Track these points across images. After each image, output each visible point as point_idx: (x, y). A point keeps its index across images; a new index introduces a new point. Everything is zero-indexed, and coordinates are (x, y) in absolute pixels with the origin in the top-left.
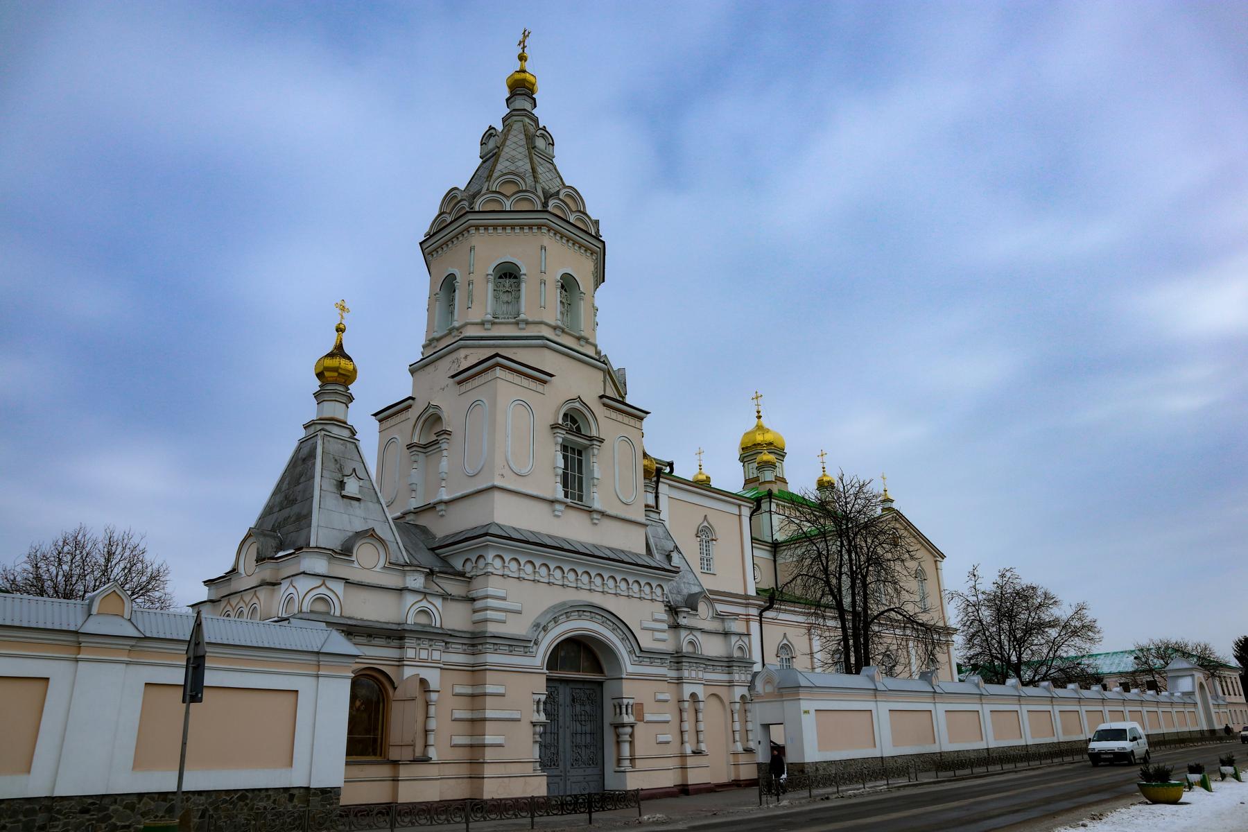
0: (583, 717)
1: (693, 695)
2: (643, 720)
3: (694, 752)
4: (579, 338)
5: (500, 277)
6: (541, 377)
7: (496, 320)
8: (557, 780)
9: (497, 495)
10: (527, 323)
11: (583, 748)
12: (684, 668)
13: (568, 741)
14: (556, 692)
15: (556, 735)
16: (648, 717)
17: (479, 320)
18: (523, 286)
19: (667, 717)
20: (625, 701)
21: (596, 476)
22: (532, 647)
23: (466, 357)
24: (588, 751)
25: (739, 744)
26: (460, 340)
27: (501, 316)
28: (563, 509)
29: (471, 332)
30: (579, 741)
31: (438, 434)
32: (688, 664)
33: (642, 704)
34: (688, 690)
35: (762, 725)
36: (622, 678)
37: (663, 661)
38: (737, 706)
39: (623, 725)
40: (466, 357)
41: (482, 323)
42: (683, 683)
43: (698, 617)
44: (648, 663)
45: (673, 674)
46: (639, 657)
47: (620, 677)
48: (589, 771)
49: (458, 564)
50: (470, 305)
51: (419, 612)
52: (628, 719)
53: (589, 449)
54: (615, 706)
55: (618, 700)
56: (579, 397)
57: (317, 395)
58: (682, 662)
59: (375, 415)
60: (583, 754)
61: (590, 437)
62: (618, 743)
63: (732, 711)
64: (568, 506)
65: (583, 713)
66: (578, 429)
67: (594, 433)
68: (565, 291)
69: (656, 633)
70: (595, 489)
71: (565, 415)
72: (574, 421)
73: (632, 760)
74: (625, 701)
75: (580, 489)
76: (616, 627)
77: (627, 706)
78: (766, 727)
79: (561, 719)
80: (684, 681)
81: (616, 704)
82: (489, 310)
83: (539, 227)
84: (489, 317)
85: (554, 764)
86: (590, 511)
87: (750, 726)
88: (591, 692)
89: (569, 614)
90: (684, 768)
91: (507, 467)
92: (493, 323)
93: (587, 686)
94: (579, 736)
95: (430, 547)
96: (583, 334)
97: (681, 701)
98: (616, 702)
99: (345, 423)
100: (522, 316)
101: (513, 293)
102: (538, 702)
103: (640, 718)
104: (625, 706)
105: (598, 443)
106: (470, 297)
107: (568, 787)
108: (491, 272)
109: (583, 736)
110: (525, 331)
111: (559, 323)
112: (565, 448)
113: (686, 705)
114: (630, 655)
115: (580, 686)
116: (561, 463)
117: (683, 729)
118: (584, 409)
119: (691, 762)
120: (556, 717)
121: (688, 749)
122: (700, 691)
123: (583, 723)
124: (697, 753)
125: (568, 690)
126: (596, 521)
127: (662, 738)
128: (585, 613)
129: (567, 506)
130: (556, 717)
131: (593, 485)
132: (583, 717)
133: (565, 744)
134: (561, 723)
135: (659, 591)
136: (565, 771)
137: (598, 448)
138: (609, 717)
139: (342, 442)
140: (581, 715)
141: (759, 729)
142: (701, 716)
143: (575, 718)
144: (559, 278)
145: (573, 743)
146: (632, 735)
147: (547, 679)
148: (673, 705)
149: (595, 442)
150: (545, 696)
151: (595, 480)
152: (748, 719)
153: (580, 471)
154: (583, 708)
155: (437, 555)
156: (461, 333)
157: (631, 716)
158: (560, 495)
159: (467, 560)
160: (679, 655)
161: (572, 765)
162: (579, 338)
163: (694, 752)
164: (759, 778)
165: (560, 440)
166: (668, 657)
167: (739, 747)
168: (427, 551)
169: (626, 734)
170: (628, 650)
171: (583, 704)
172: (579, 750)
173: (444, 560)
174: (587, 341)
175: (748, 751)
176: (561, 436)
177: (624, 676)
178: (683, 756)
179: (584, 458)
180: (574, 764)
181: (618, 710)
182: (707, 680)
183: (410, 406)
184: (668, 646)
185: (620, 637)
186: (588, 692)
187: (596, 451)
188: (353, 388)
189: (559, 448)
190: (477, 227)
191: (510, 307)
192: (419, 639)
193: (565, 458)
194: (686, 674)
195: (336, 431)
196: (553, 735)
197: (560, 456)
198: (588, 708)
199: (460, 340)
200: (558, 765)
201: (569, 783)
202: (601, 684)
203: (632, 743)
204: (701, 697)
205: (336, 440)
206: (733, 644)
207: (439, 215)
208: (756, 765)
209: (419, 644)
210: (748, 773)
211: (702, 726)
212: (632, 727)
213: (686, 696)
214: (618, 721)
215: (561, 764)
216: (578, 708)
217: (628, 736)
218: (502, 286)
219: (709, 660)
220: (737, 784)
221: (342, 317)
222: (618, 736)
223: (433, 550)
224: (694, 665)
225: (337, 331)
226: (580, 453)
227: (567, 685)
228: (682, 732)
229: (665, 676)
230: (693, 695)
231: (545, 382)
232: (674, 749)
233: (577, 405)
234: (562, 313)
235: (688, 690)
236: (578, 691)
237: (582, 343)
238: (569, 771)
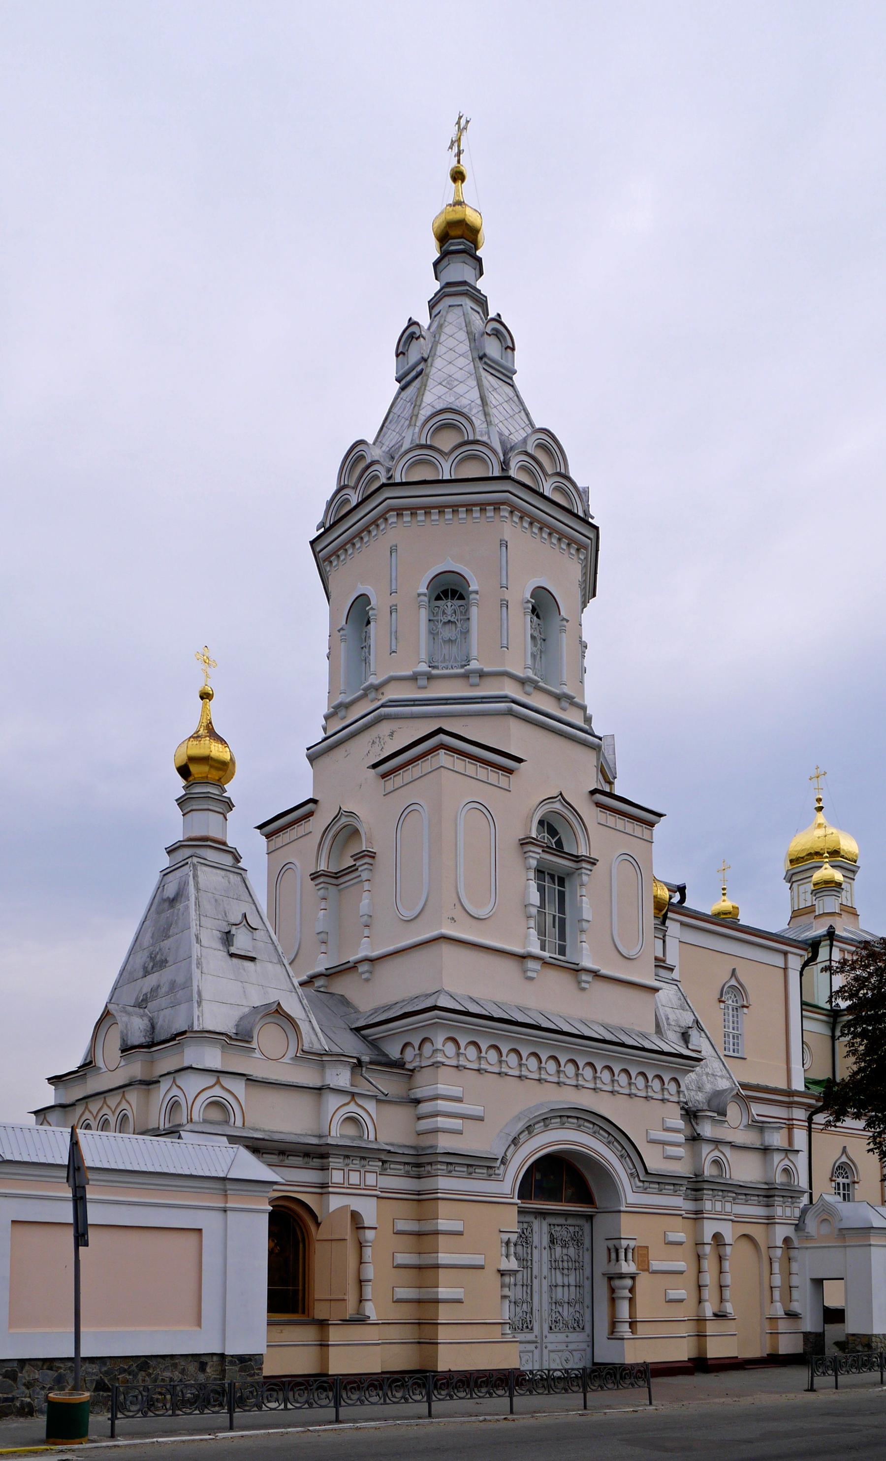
0: (565, 1264)
1: (717, 1237)
2: (647, 1270)
3: (715, 1315)
4: (559, 698)
7: (435, 672)
8: (531, 1347)
9: (447, 951)
11: (566, 1306)
12: (705, 1197)
13: (545, 1297)
14: (529, 1230)
15: (529, 1288)
16: (655, 1265)
17: (408, 673)
19: (681, 1265)
20: (624, 1243)
21: (585, 917)
22: (498, 1168)
23: (392, 735)
24: (571, 1310)
25: (778, 1305)
26: (382, 706)
27: (440, 665)
28: (539, 968)
29: (393, 693)
30: (559, 1296)
31: (357, 857)
32: (710, 1192)
33: (647, 1247)
34: (709, 1229)
35: (812, 1280)
36: (620, 1212)
37: (677, 1187)
38: (779, 1252)
39: (621, 1276)
40: (392, 735)
41: (414, 678)
42: (704, 1218)
43: (726, 1125)
44: (655, 1191)
45: (689, 1205)
46: (643, 1182)
47: (616, 1209)
48: (573, 1337)
49: (394, 1052)
50: (394, 648)
51: (347, 1118)
52: (627, 1267)
53: (576, 875)
54: (609, 1250)
55: (615, 1242)
56: (561, 794)
57: (182, 802)
58: (703, 1189)
60: (565, 1314)
61: (577, 857)
62: (613, 1301)
63: (771, 1259)
64: (545, 963)
65: (565, 1258)
66: (559, 843)
67: (583, 851)
69: (665, 1147)
70: (584, 937)
71: (541, 823)
73: (632, 1324)
74: (624, 1243)
75: (562, 936)
76: (613, 1139)
77: (626, 1250)
78: (818, 1283)
79: (536, 1266)
80: (705, 1215)
81: (611, 1246)
82: (423, 656)
84: (423, 667)
85: (527, 1327)
86: (576, 970)
87: (795, 1280)
88: (577, 1229)
89: (547, 1122)
90: (701, 1336)
91: (458, 906)
92: (430, 677)
93: (570, 1221)
94: (560, 1289)
95: (353, 1026)
97: (699, 1244)
98: (611, 1244)
99: (224, 844)
101: (459, 625)
102: (508, 1243)
103: (644, 1266)
104: (623, 1250)
105: (589, 866)
106: (395, 634)
107: (545, 1357)
109: (566, 1289)
110: (478, 688)
112: (540, 872)
113: (708, 1249)
114: (632, 1179)
115: (561, 1221)
116: (535, 897)
117: (701, 1284)
119: (711, 1328)
120: (529, 1263)
121: (709, 1310)
122: (728, 1232)
123: (566, 1271)
124: (720, 1316)
125: (545, 1228)
126: (584, 985)
127: (674, 1294)
128: (570, 1120)
129: (545, 963)
130: (529, 1263)
131: (582, 931)
132: (565, 1264)
133: (541, 1301)
134: (535, 1272)
135: (672, 1087)
136: (542, 1339)
137: (588, 872)
138: (602, 1265)
139: (223, 873)
140: (562, 1261)
141: (808, 1285)
142: (727, 1265)
143: (555, 1265)
144: (528, 596)
145: (552, 1298)
146: (632, 1290)
147: (519, 1212)
148: (688, 1250)
149: (584, 865)
150: (516, 1235)
151: (584, 923)
152: (794, 1270)
153: (562, 909)
154: (565, 1251)
155: (364, 1037)
156: (383, 694)
157: (631, 1263)
160: (700, 1179)
162: (559, 698)
163: (715, 1315)
164: (805, 1353)
165: (533, 863)
166: (685, 1182)
167: (779, 1309)
168: (349, 1030)
169: (624, 1288)
170: (629, 1171)
171: (565, 1246)
172: (560, 1309)
173: (373, 1044)
174: (569, 699)
175: (792, 1315)
176: (535, 856)
177: (623, 1209)
178: (700, 1321)
179: (567, 890)
180: (553, 1327)
181: (613, 1255)
182: (736, 1215)
183: (311, 814)
184: (682, 1168)
185: (619, 1154)
186: (571, 1229)
187: (585, 878)
188: (231, 789)
189: (532, 875)
191: (454, 649)
192: (347, 1157)
193: (541, 889)
194: (708, 1205)
195: (211, 855)
196: (525, 1288)
197: (533, 885)
198: (572, 1251)
199: (382, 706)
200: (532, 1329)
201: (545, 1352)
202: (590, 1218)
203: (631, 1300)
204: (728, 1238)
205: (215, 871)
206: (775, 1164)
208: (802, 1335)
209: (347, 1165)
210: (788, 1345)
211: (728, 1279)
212: (633, 1278)
213: (708, 1238)
214: (613, 1269)
216: (558, 1250)
217: (627, 1291)
218: (440, 613)
219: (741, 1186)
220: (774, 1360)
221: (207, 676)
222: (612, 1290)
223: (358, 1030)
224: (720, 1193)
225: (202, 698)
226: (562, 882)
228: (700, 1287)
229: (678, 1208)
230: (717, 1237)
232: (687, 1311)
233: (557, 806)
234: (534, 656)
235: (709, 1229)
236: (558, 1228)
238: (546, 1337)
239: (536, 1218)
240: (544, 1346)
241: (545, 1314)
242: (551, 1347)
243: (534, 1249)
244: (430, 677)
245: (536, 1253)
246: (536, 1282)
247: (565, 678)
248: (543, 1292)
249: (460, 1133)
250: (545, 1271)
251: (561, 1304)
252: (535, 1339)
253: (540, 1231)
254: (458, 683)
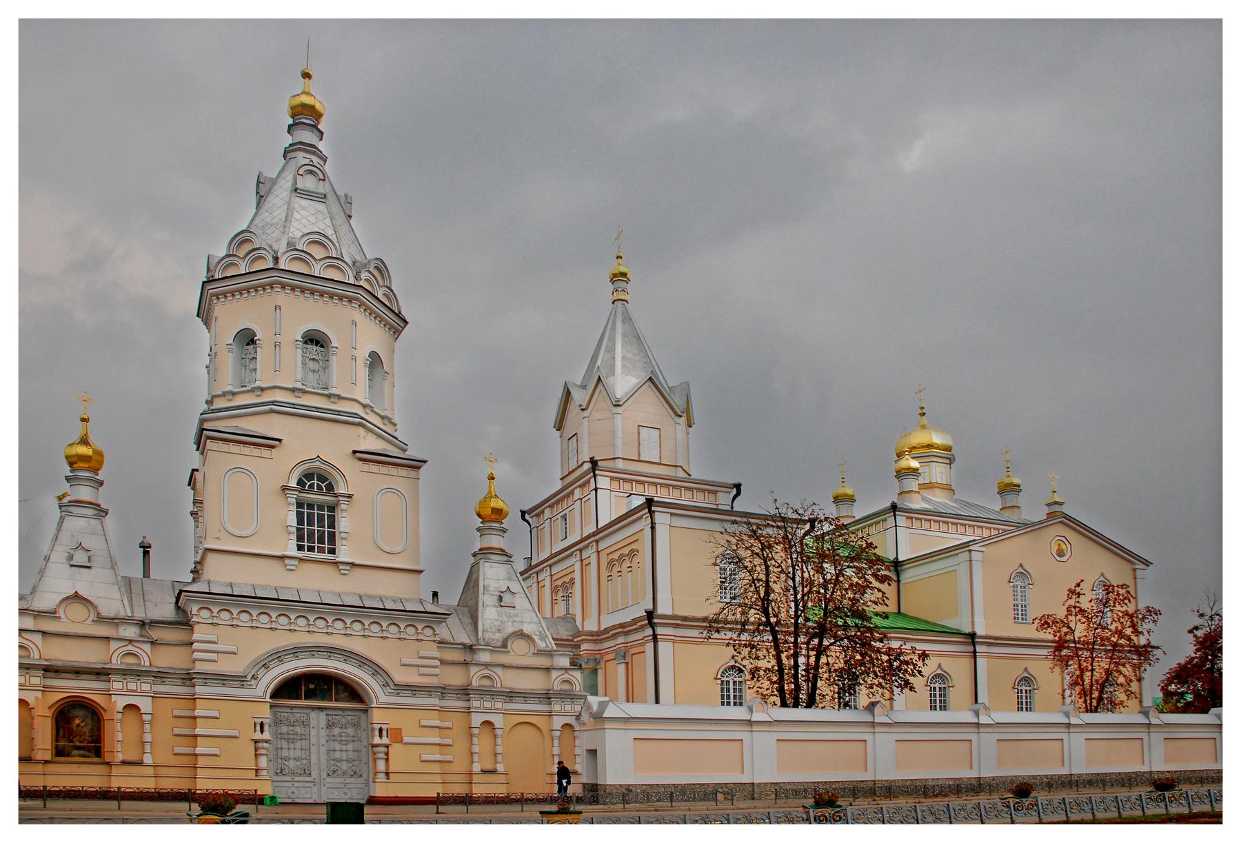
8: (312, 785)
13: (324, 758)
56: (318, 456)
66: (330, 488)
72: (322, 478)
85: (305, 773)
86: (336, 564)
118: (328, 468)
149: (340, 498)
158: (295, 553)
161: (328, 775)
162: (329, 396)
172: (339, 764)
174: (339, 397)
187: (343, 507)
201: (324, 789)
215: (315, 774)
216: (337, 731)
226: (332, 508)
227: (322, 711)
233: (318, 464)
236: (338, 717)
239: (313, 711)
240: (322, 784)
241: (325, 767)
242: (328, 785)
243: (311, 729)
245: (313, 732)
246: (313, 749)
247: (334, 384)
248: (321, 753)
249: (215, 661)
250: (323, 741)
251: (338, 761)
252: (312, 780)
253: (318, 720)
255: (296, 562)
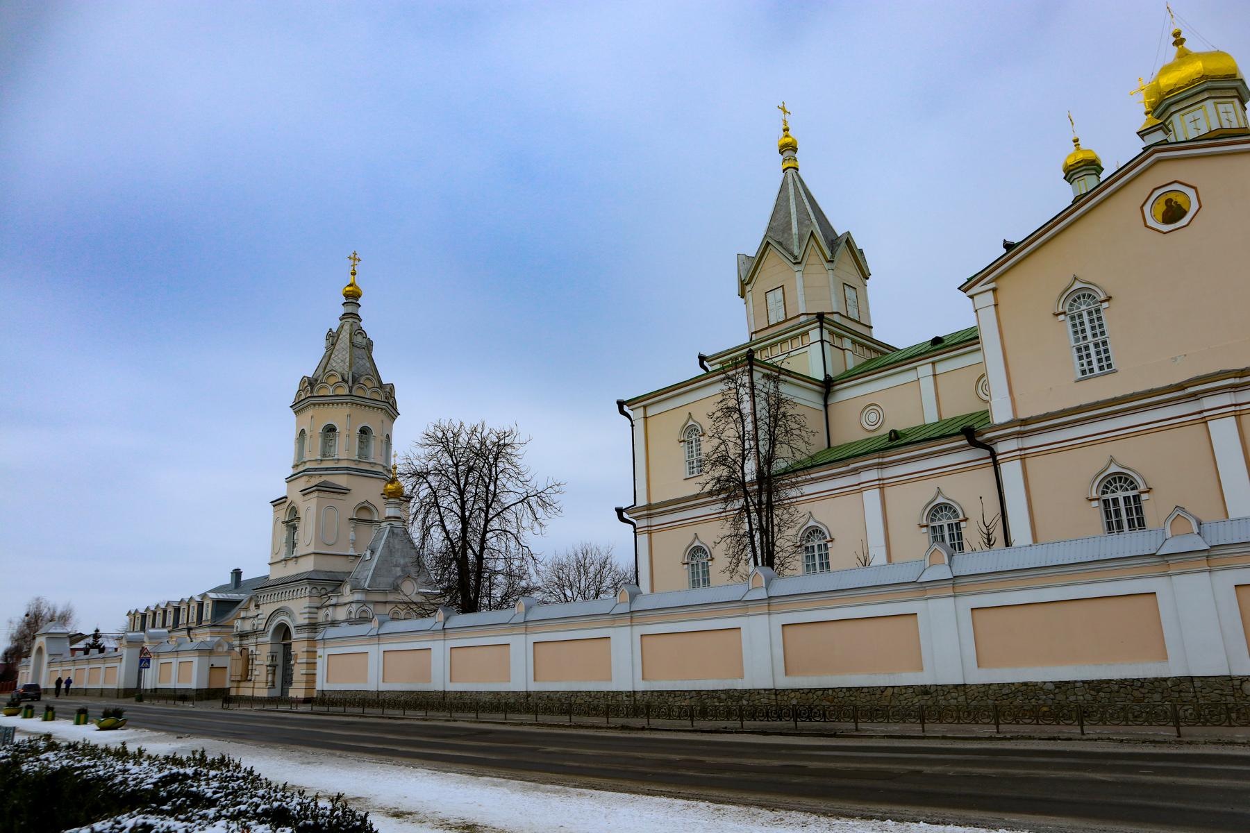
4: (370, 463)
5: (328, 432)
6: (343, 491)
10: (338, 460)
17: (313, 459)
18: (337, 438)
41: (316, 460)
59: (272, 502)
68: (366, 434)
83: (347, 403)
84: (319, 457)
96: (372, 461)
100: (336, 457)
108: (321, 431)
111: (357, 458)
159: (302, 589)
174: (375, 464)
190: (314, 405)
207: (299, 390)
231: (346, 494)
237: (372, 465)
244: (321, 460)
254: (333, 462)
255: (353, 558)
